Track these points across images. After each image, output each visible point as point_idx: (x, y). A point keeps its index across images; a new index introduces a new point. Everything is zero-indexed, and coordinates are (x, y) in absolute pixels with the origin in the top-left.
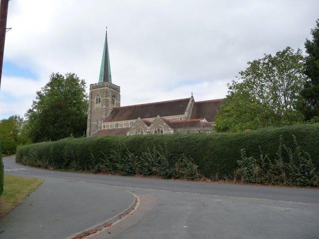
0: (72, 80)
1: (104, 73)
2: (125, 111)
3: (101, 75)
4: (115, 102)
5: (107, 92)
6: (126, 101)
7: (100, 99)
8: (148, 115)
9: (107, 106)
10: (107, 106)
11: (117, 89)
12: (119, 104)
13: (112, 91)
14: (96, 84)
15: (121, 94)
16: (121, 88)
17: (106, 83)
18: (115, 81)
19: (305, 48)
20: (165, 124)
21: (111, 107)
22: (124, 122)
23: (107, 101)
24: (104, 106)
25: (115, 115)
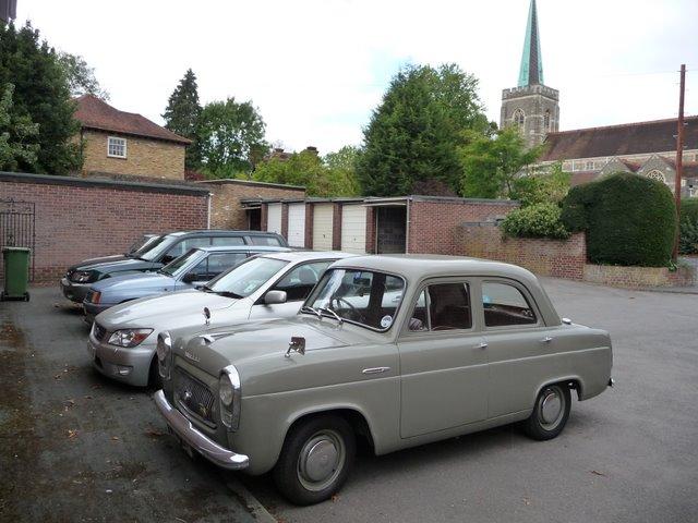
0: (454, 85)
1: (531, 66)
2: (574, 141)
3: (523, 71)
4: (551, 121)
5: (537, 104)
6: (569, 121)
7: (522, 118)
8: (624, 149)
9: (537, 130)
10: (537, 130)
11: (552, 95)
12: (557, 126)
13: (547, 102)
14: (514, 89)
15: (560, 104)
16: (561, 97)
17: (536, 86)
18: (549, 79)
19: (231, 101)
20: (668, 169)
21: (544, 131)
22: (573, 162)
23: (537, 121)
24: (532, 132)
25: (552, 149)
